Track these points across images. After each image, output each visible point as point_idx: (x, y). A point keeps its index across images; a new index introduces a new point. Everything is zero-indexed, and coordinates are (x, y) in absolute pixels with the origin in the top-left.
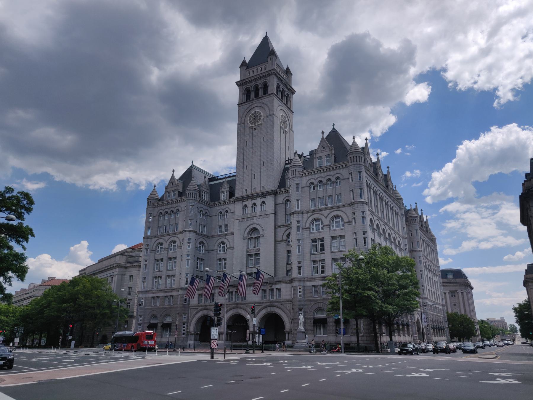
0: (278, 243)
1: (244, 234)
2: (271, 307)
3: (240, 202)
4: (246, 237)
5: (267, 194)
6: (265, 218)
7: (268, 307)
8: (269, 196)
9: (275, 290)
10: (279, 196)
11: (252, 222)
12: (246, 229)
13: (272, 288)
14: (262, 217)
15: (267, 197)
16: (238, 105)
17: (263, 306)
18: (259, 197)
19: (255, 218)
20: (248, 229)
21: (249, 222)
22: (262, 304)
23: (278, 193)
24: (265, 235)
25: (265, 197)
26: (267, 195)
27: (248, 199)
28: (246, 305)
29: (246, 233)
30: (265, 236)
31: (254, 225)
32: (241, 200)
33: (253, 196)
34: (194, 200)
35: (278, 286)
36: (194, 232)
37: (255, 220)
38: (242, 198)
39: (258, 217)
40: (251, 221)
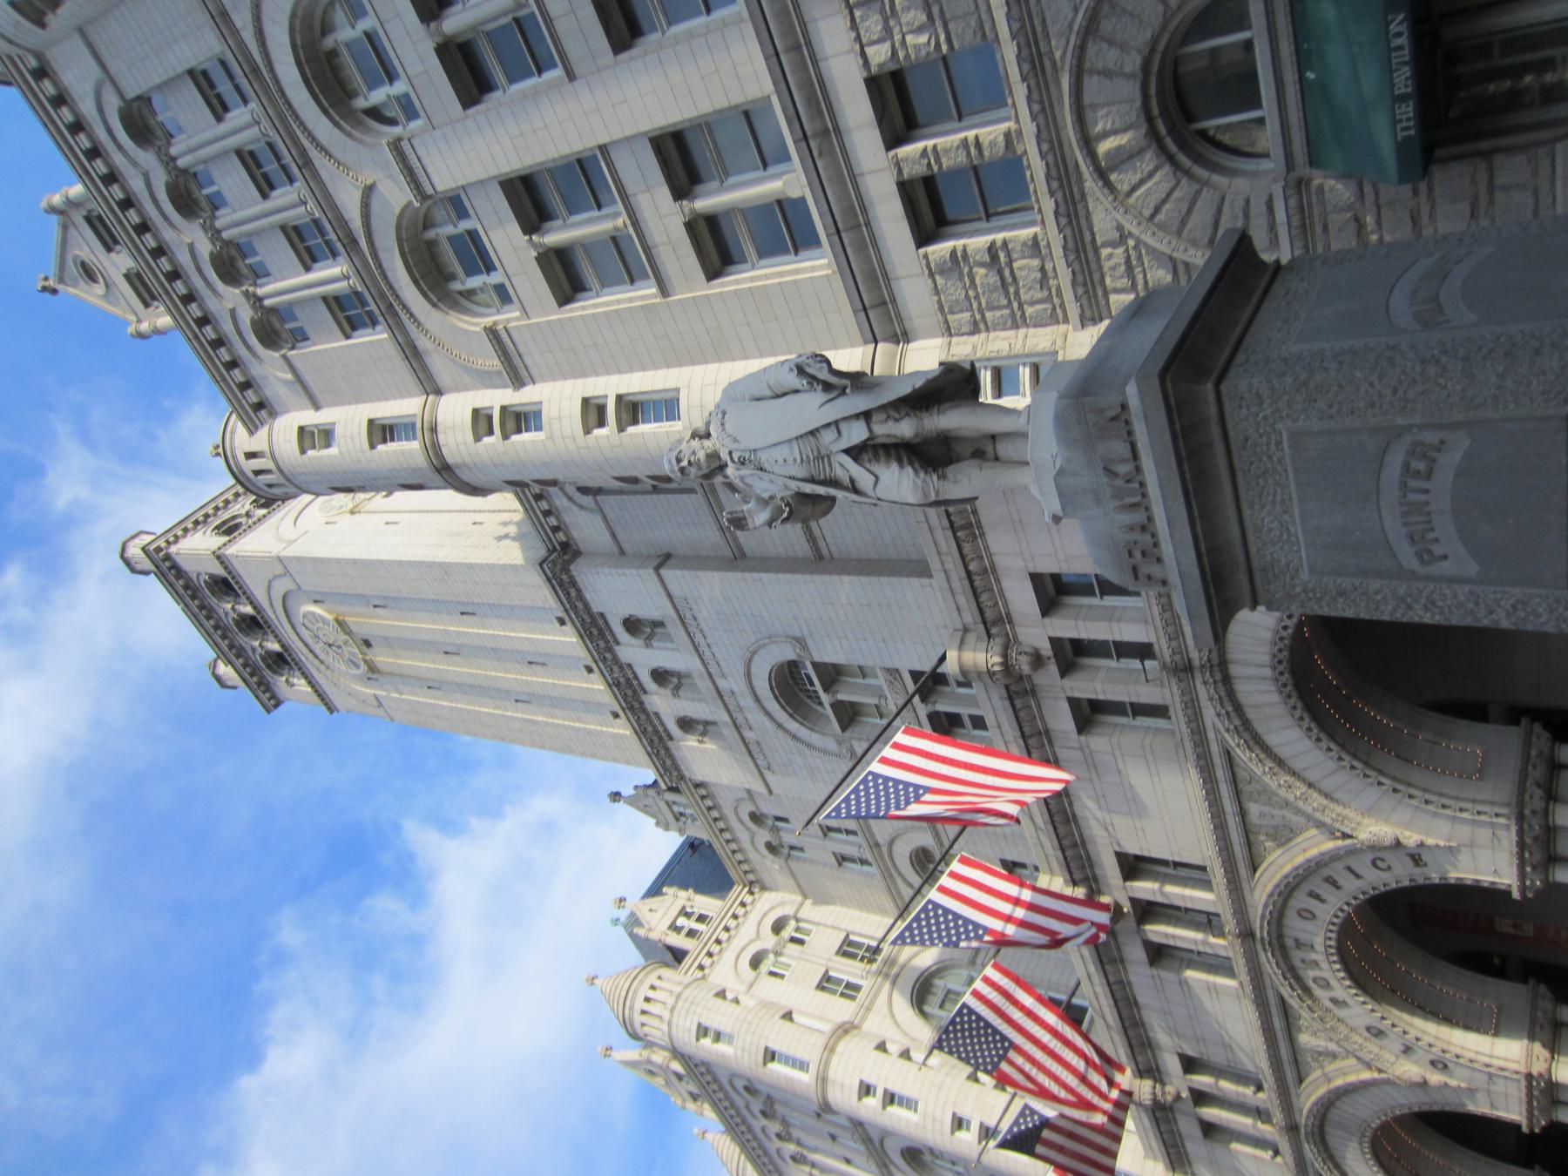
0: (821, 543)
1: (826, 752)
2: (1234, 670)
3: (675, 753)
4: (840, 743)
5: (579, 604)
6: (706, 630)
7: (1231, 693)
8: (588, 597)
9: (1067, 627)
10: (575, 534)
11: (747, 701)
12: (794, 737)
13: (1046, 649)
14: (699, 638)
15: (596, 608)
16: (332, 712)
17: (1231, 741)
18: (610, 650)
19: (722, 683)
20: (792, 725)
21: (755, 716)
22: (1215, 749)
23: (561, 537)
24: (790, 634)
25: (602, 615)
26: (587, 606)
27: (644, 711)
28: (1243, 871)
29: (815, 738)
30: (798, 634)
31: (759, 692)
32: (667, 749)
33: (618, 685)
34: (672, 1011)
35: (1021, 599)
36: (832, 1050)
37: (733, 683)
38: (651, 742)
39: (714, 669)
40: (742, 703)
